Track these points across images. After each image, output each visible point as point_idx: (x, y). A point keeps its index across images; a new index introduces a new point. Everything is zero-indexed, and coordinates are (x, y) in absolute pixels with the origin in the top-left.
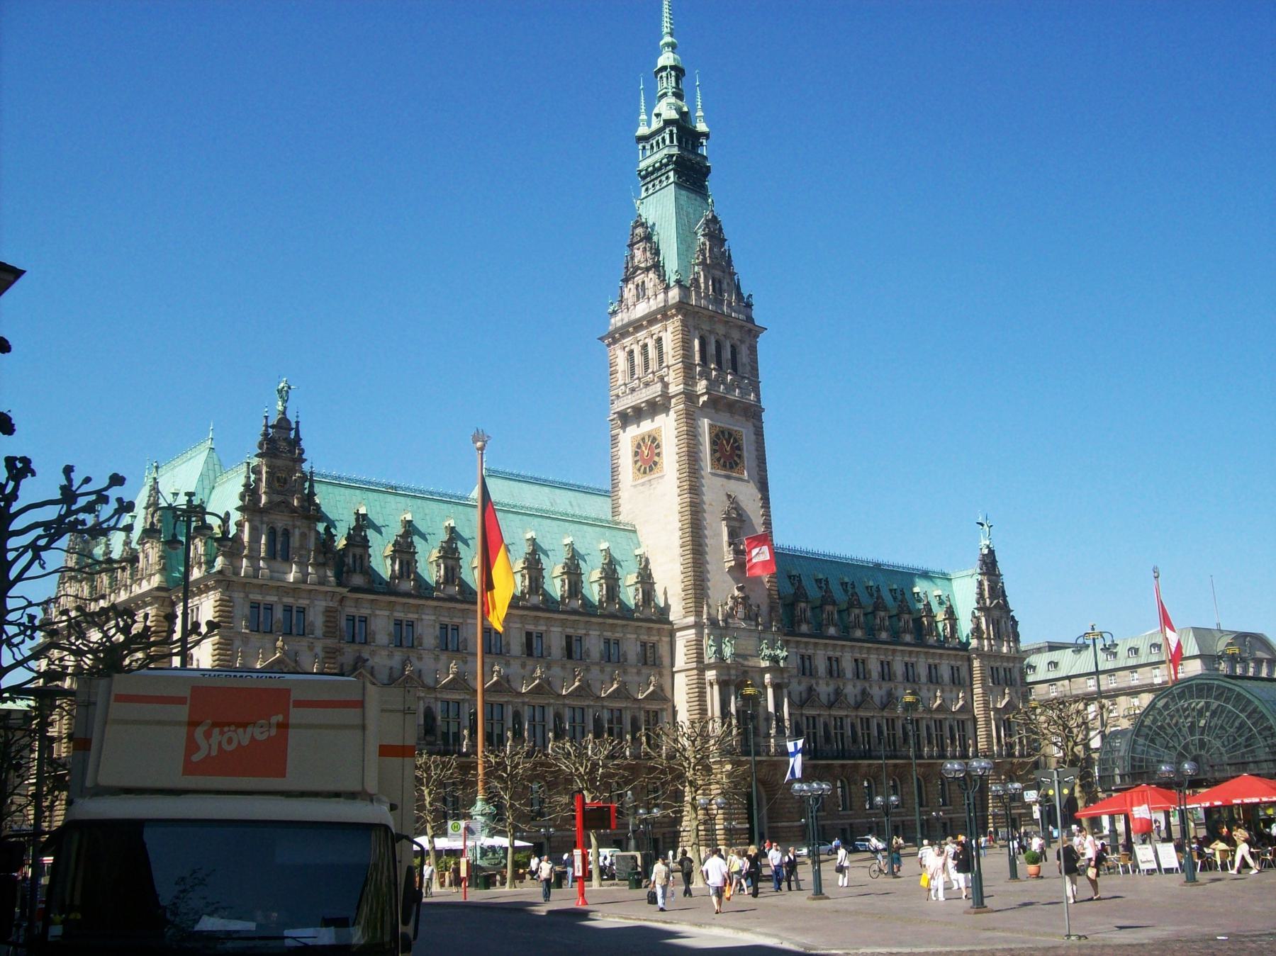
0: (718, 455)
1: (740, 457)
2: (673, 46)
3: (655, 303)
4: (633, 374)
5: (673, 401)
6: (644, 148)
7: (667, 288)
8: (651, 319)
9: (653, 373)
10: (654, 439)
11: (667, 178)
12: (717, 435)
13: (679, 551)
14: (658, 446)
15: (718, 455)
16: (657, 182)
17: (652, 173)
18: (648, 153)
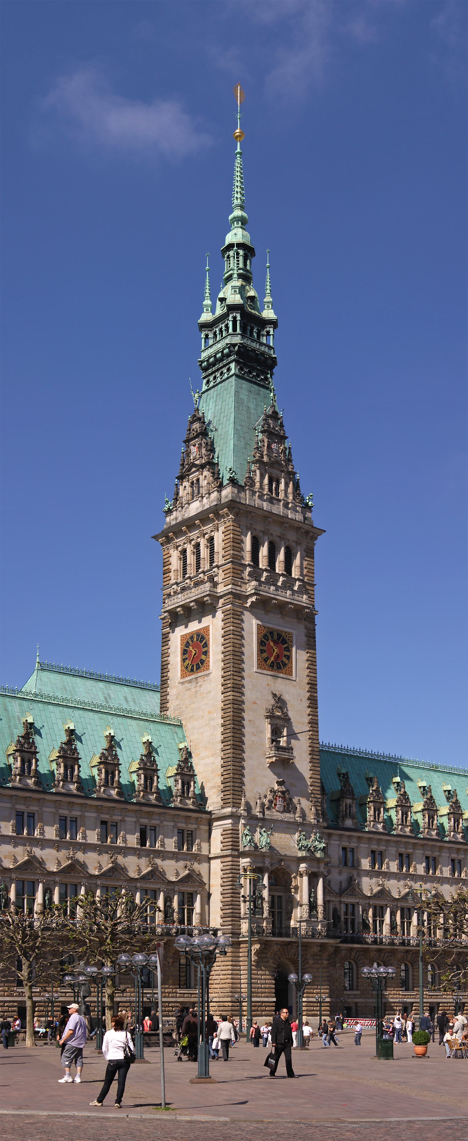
0: (265, 655)
1: (289, 658)
2: (243, 221)
3: (208, 502)
4: (185, 572)
5: (221, 601)
6: (207, 336)
7: (221, 487)
8: (203, 518)
9: (203, 572)
10: (203, 638)
11: (229, 370)
12: (265, 636)
13: (220, 746)
14: (206, 645)
15: (265, 655)
16: (218, 374)
17: (214, 364)
18: (211, 342)
